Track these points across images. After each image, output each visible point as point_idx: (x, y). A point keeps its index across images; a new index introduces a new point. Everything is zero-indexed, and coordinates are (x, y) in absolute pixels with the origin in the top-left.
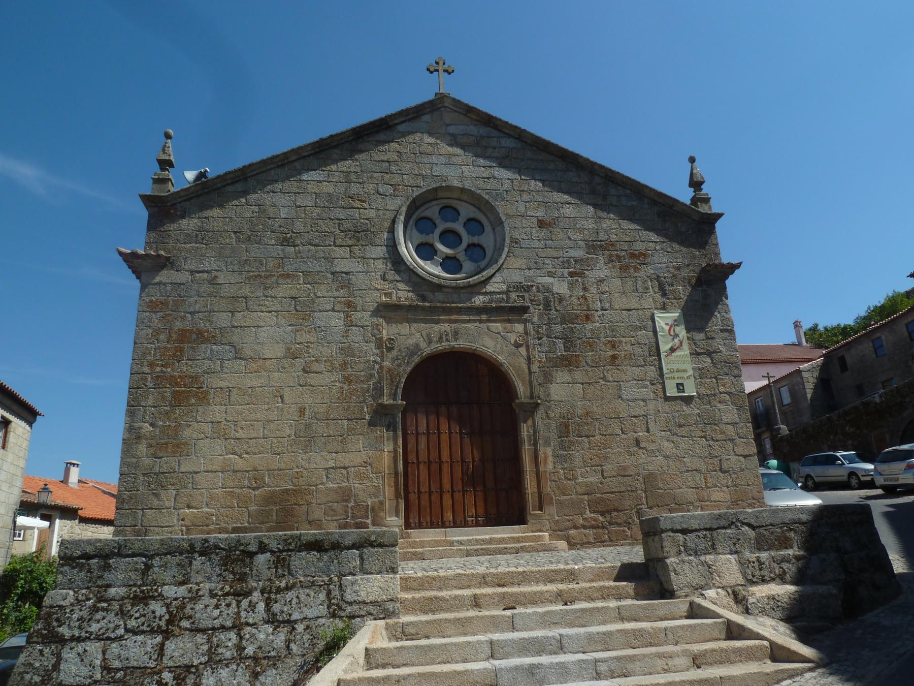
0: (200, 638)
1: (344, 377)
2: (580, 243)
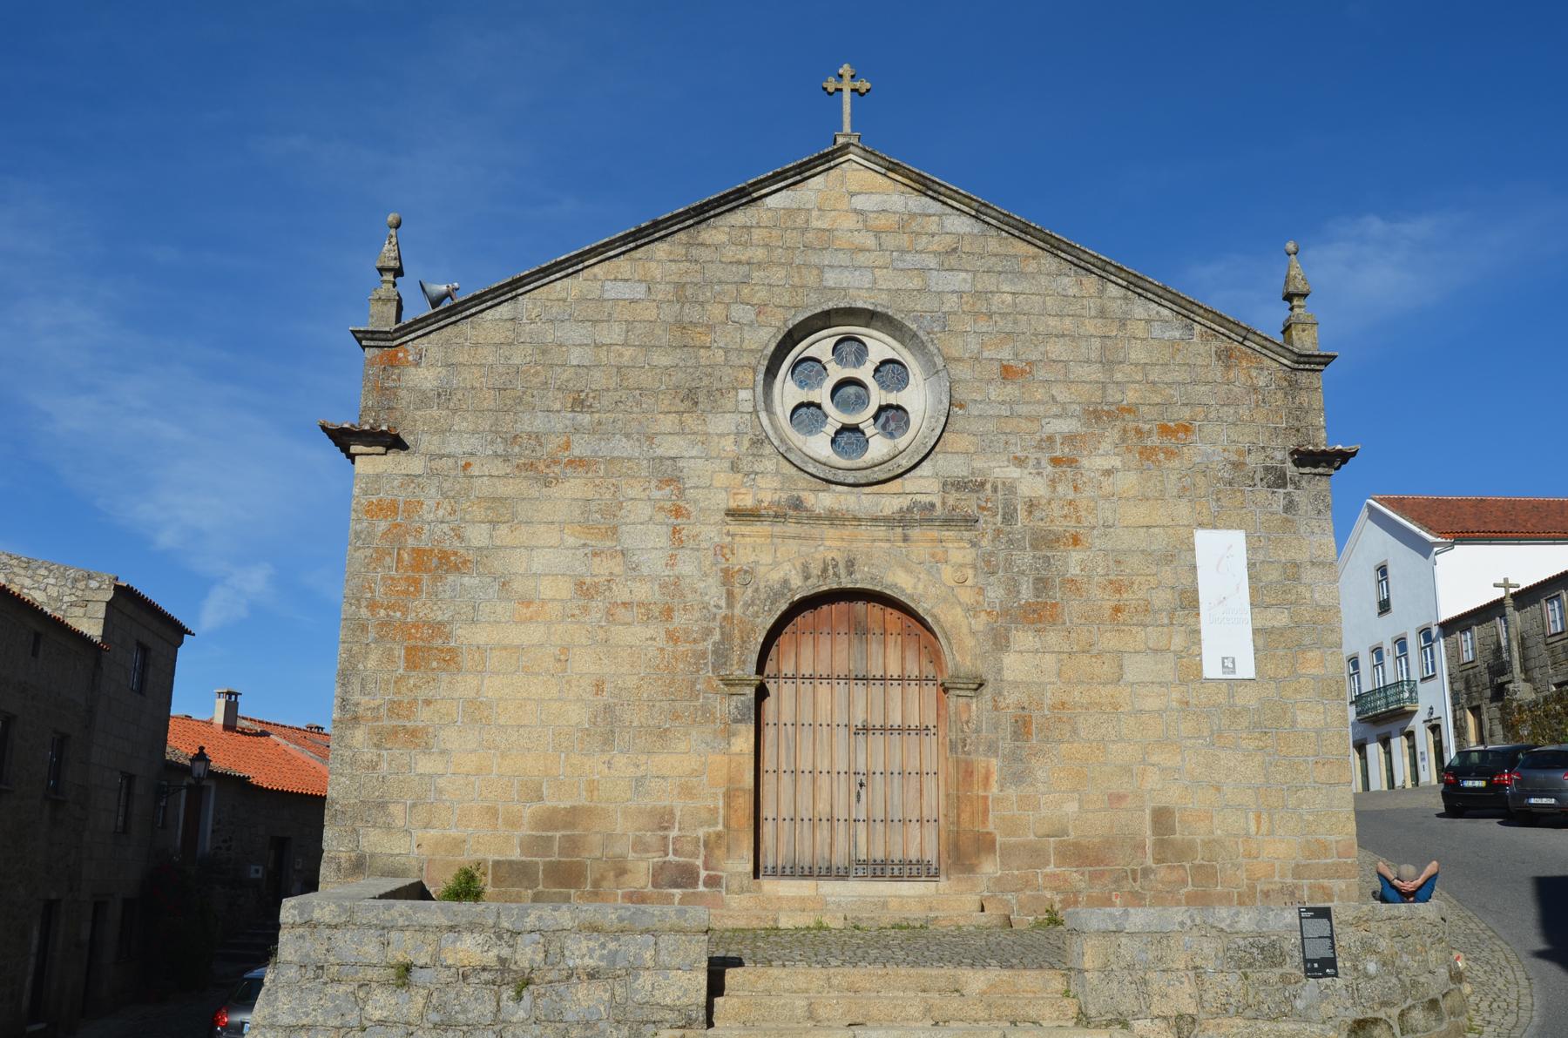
1: (667, 632)
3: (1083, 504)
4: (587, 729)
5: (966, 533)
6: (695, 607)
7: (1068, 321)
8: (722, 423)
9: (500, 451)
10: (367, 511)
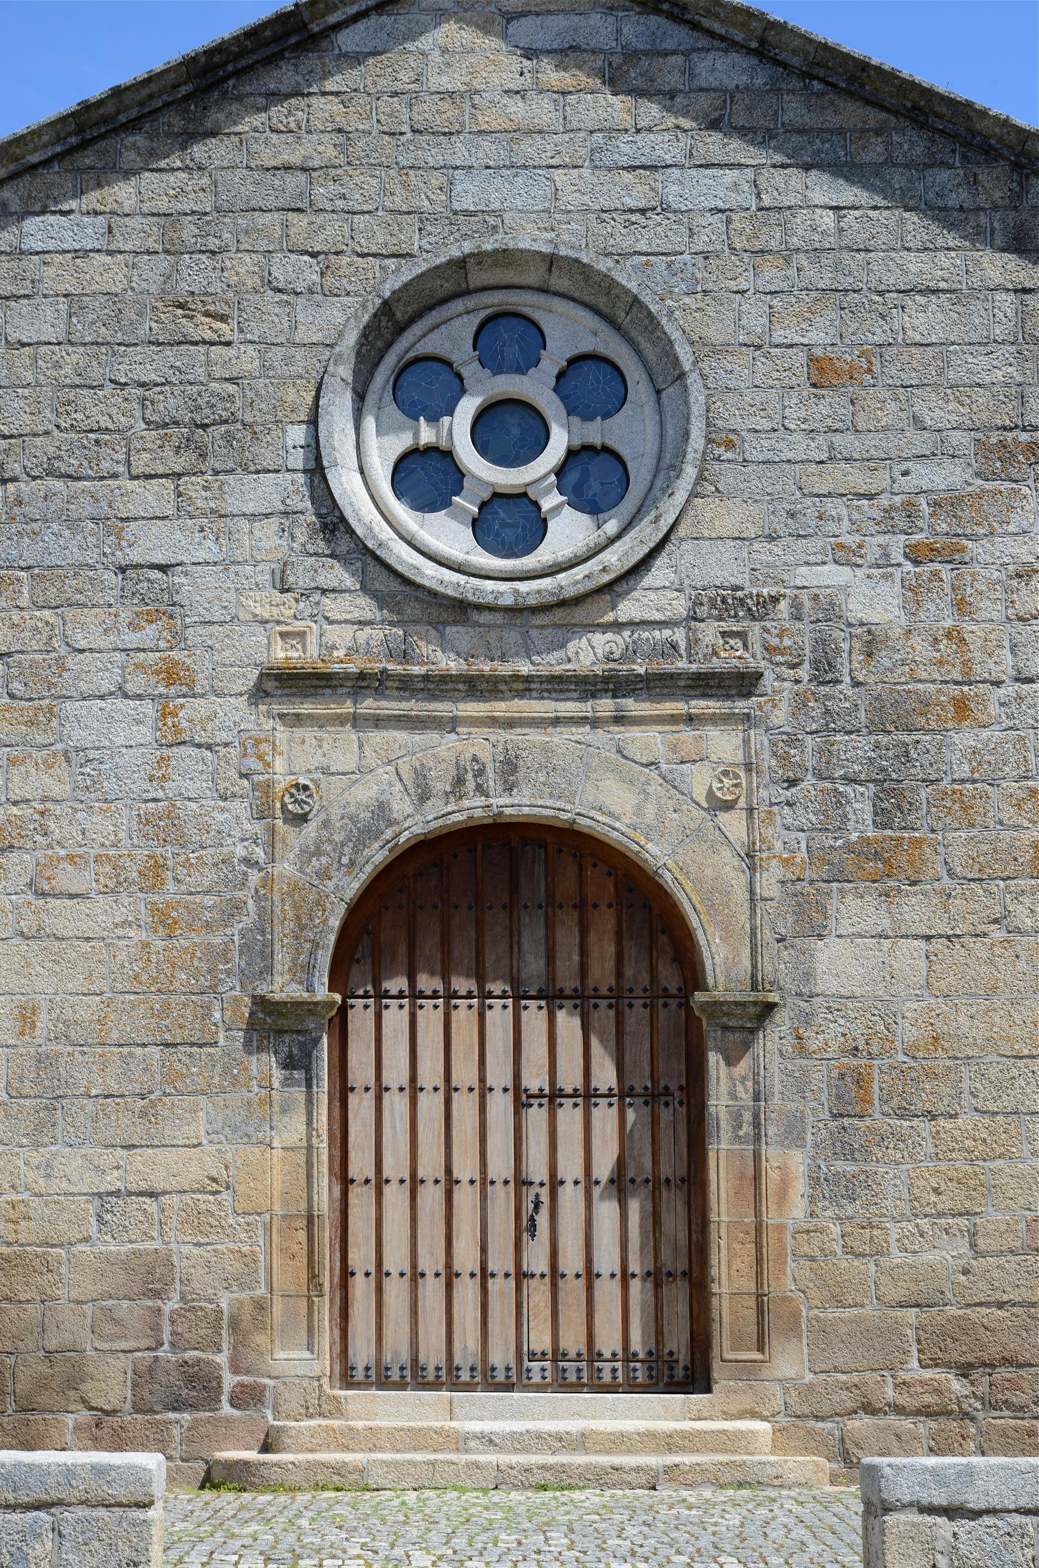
1: (154, 909)
2: (957, 437)
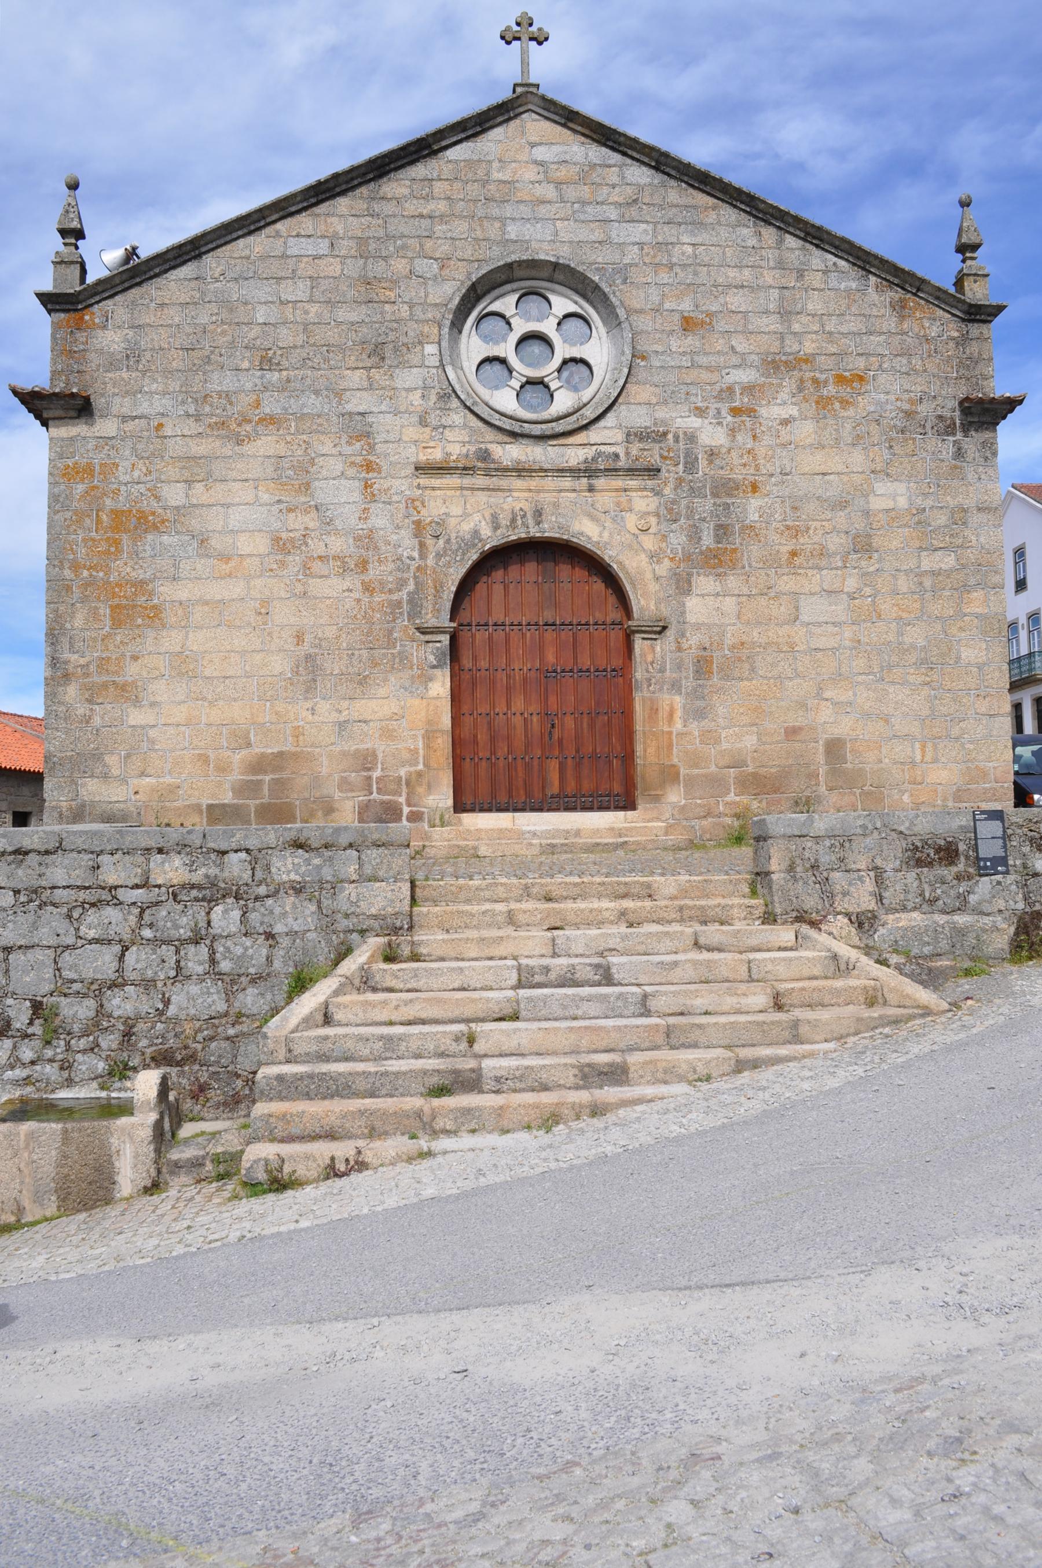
0: (167, 952)
3: (761, 451)
4: (290, 679)
5: (649, 482)
6: (390, 559)
7: (746, 272)
8: (408, 378)
9: (192, 411)
10: (64, 475)
